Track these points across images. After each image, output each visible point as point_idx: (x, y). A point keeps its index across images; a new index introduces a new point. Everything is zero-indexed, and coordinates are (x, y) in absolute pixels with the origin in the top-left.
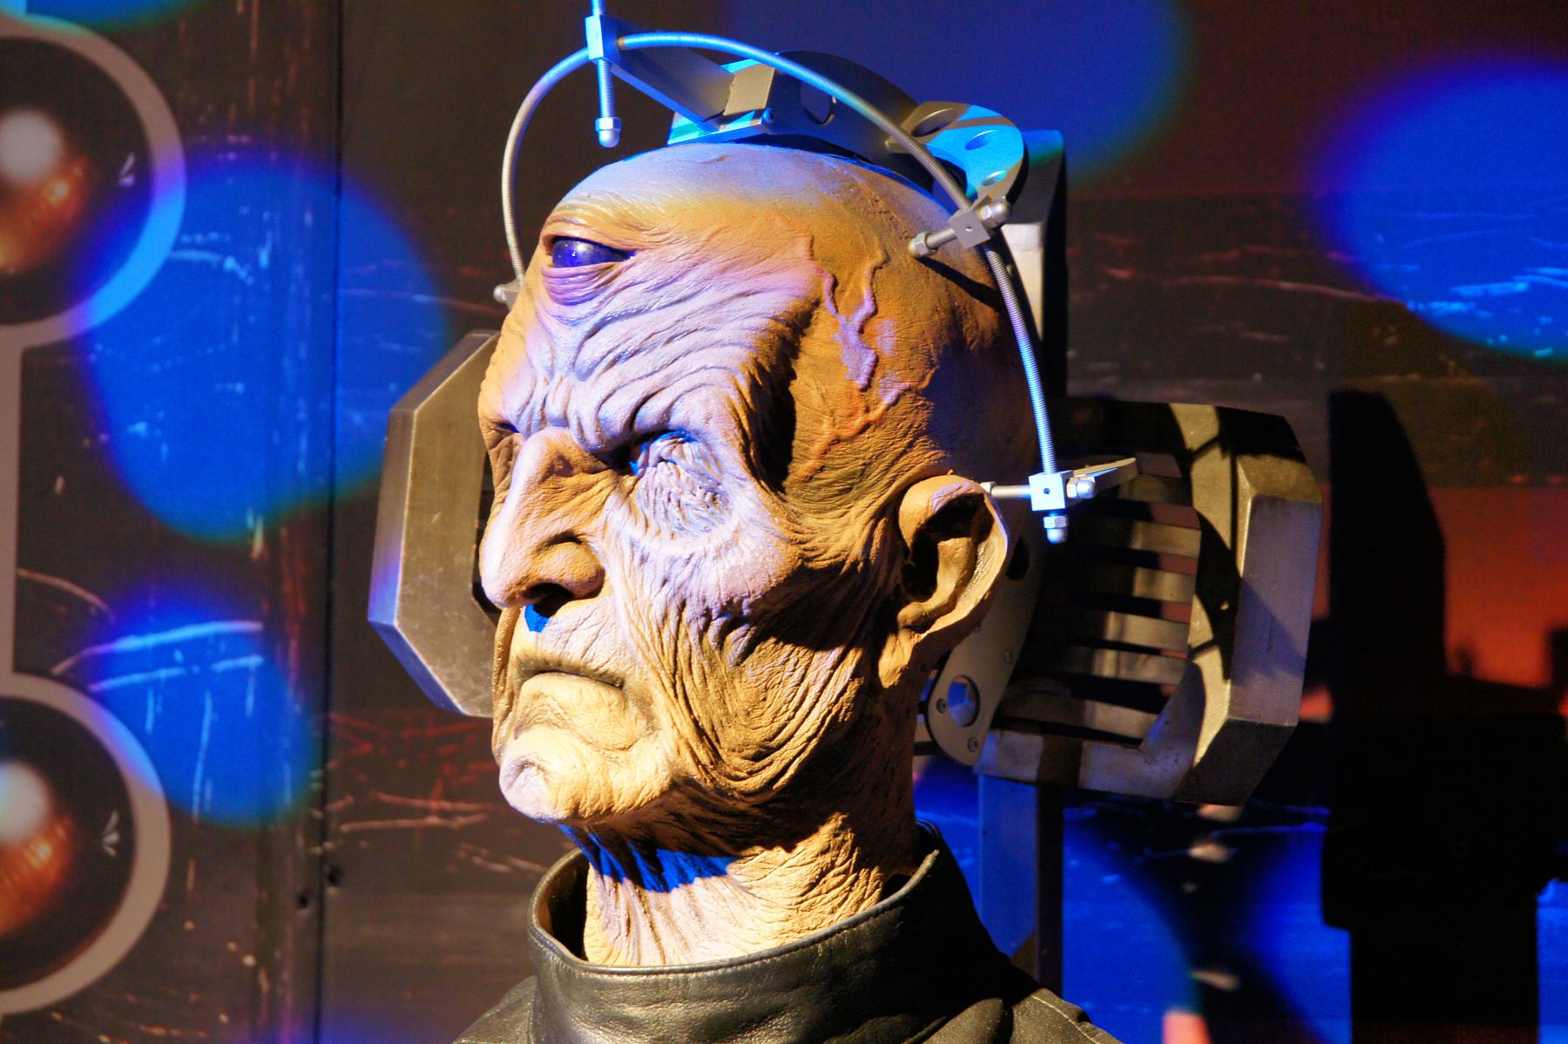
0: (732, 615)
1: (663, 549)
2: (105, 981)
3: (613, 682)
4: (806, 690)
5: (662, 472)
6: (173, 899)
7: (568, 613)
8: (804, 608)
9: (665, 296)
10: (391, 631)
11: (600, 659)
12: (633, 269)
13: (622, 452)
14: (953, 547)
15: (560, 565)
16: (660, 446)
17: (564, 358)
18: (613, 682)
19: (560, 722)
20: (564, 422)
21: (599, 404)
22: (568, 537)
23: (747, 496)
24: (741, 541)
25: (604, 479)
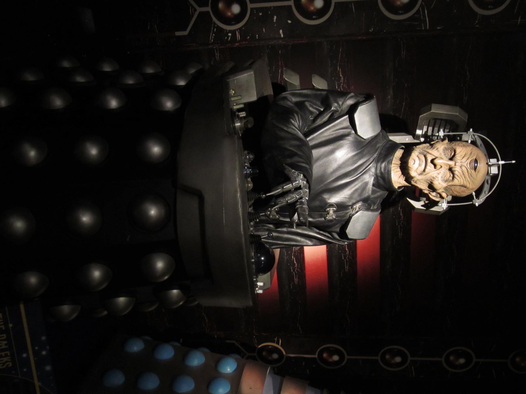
0: (432, 183)
1: (440, 176)
2: (382, 13)
3: (424, 170)
4: (423, 187)
5: (449, 175)
6: (393, 21)
7: (433, 166)
8: (431, 187)
9: (470, 175)
10: (430, 110)
11: (427, 170)
12: (473, 171)
13: (451, 170)
14: (439, 196)
15: (438, 167)
16: (452, 175)
17: (463, 164)
18: (424, 170)
19: (420, 165)
20: (455, 165)
21: (457, 170)
22: (441, 167)
23: (445, 185)
24: (440, 184)
25: (448, 168)
